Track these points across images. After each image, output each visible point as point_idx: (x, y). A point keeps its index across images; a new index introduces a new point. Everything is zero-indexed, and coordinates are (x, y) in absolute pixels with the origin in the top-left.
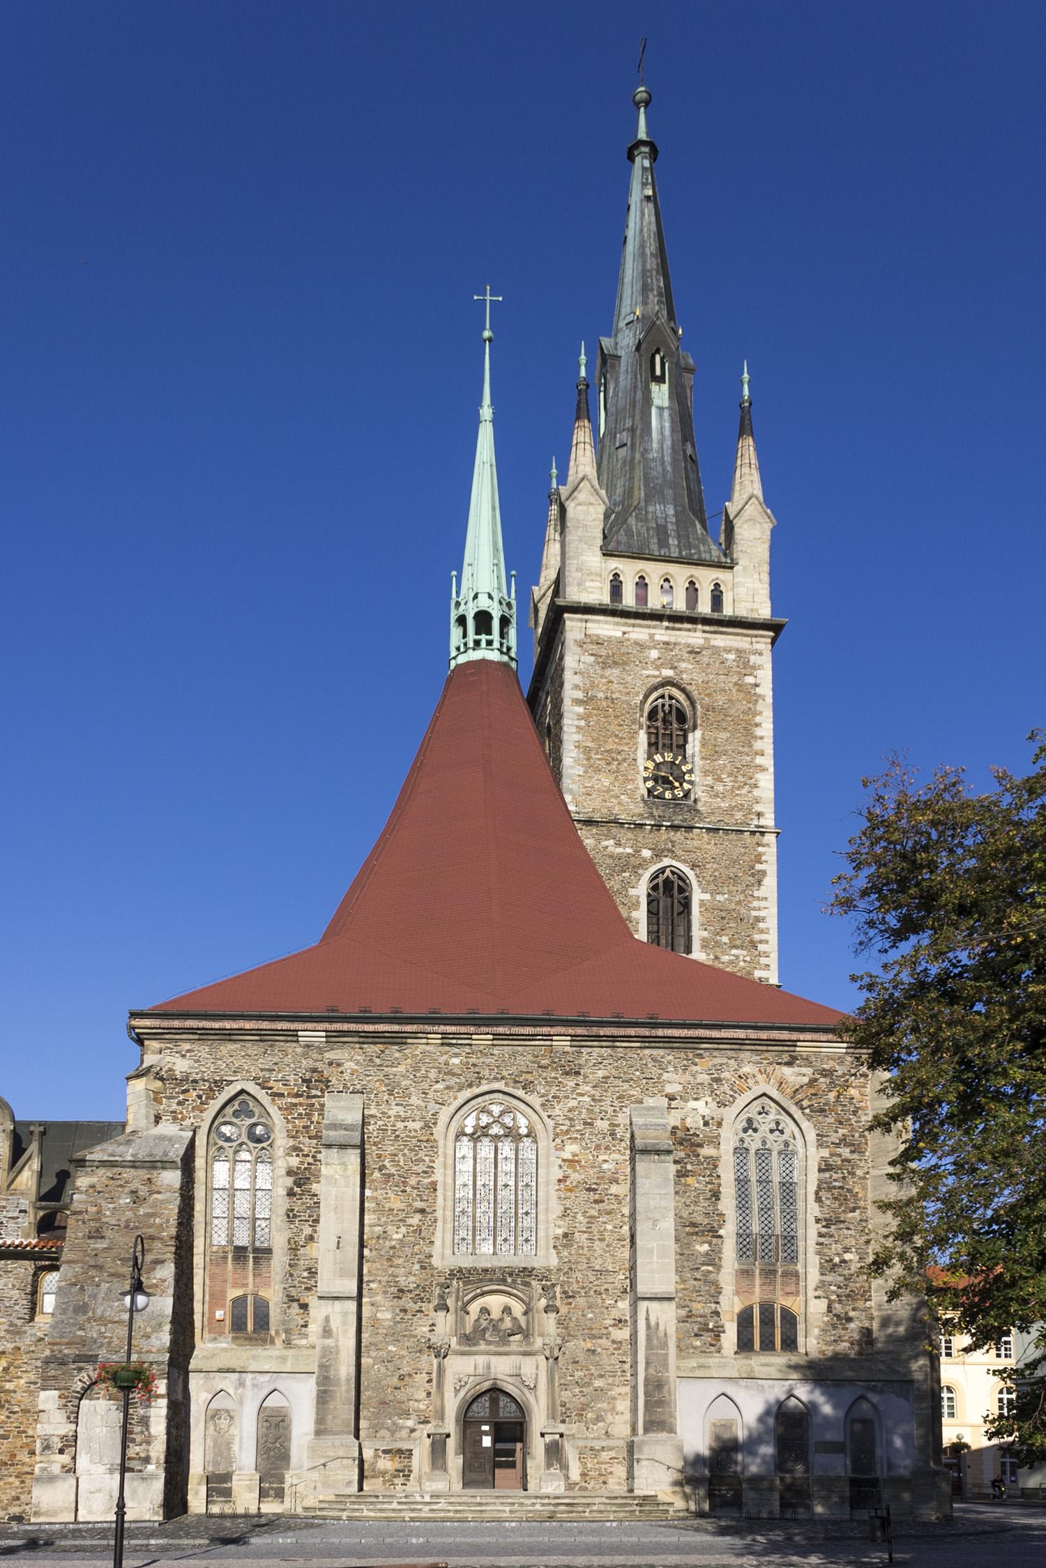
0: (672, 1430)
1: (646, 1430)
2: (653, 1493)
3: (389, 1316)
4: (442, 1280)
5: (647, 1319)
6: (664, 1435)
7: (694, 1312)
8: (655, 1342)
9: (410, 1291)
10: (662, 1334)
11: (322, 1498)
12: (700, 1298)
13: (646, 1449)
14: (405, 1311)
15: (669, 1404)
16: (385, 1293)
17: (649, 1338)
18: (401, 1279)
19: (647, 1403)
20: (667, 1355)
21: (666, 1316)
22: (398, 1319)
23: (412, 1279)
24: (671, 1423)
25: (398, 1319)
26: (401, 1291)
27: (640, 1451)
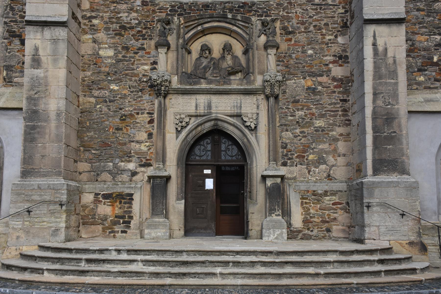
0: (404, 171)
1: (376, 172)
2: (386, 245)
3: (111, 53)
4: (163, 15)
5: (374, 45)
6: (394, 178)
7: (417, 44)
8: (383, 71)
9: (132, 28)
10: (390, 61)
11: (26, 250)
12: (424, 30)
13: (377, 192)
14: (126, 48)
15: (399, 140)
16: (107, 29)
17: (377, 67)
18: (123, 15)
19: (375, 139)
20: (396, 84)
21: (394, 41)
22: (120, 56)
23: (134, 15)
24: (403, 162)
25: (120, 56)
26: (123, 27)
27: (371, 195)
